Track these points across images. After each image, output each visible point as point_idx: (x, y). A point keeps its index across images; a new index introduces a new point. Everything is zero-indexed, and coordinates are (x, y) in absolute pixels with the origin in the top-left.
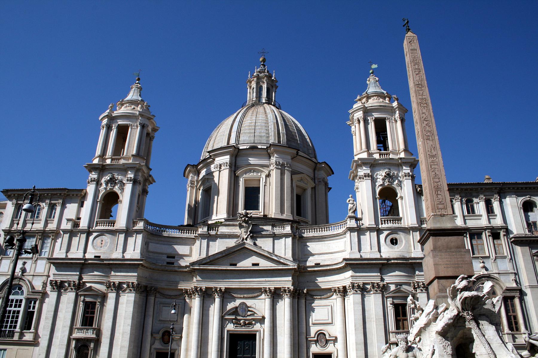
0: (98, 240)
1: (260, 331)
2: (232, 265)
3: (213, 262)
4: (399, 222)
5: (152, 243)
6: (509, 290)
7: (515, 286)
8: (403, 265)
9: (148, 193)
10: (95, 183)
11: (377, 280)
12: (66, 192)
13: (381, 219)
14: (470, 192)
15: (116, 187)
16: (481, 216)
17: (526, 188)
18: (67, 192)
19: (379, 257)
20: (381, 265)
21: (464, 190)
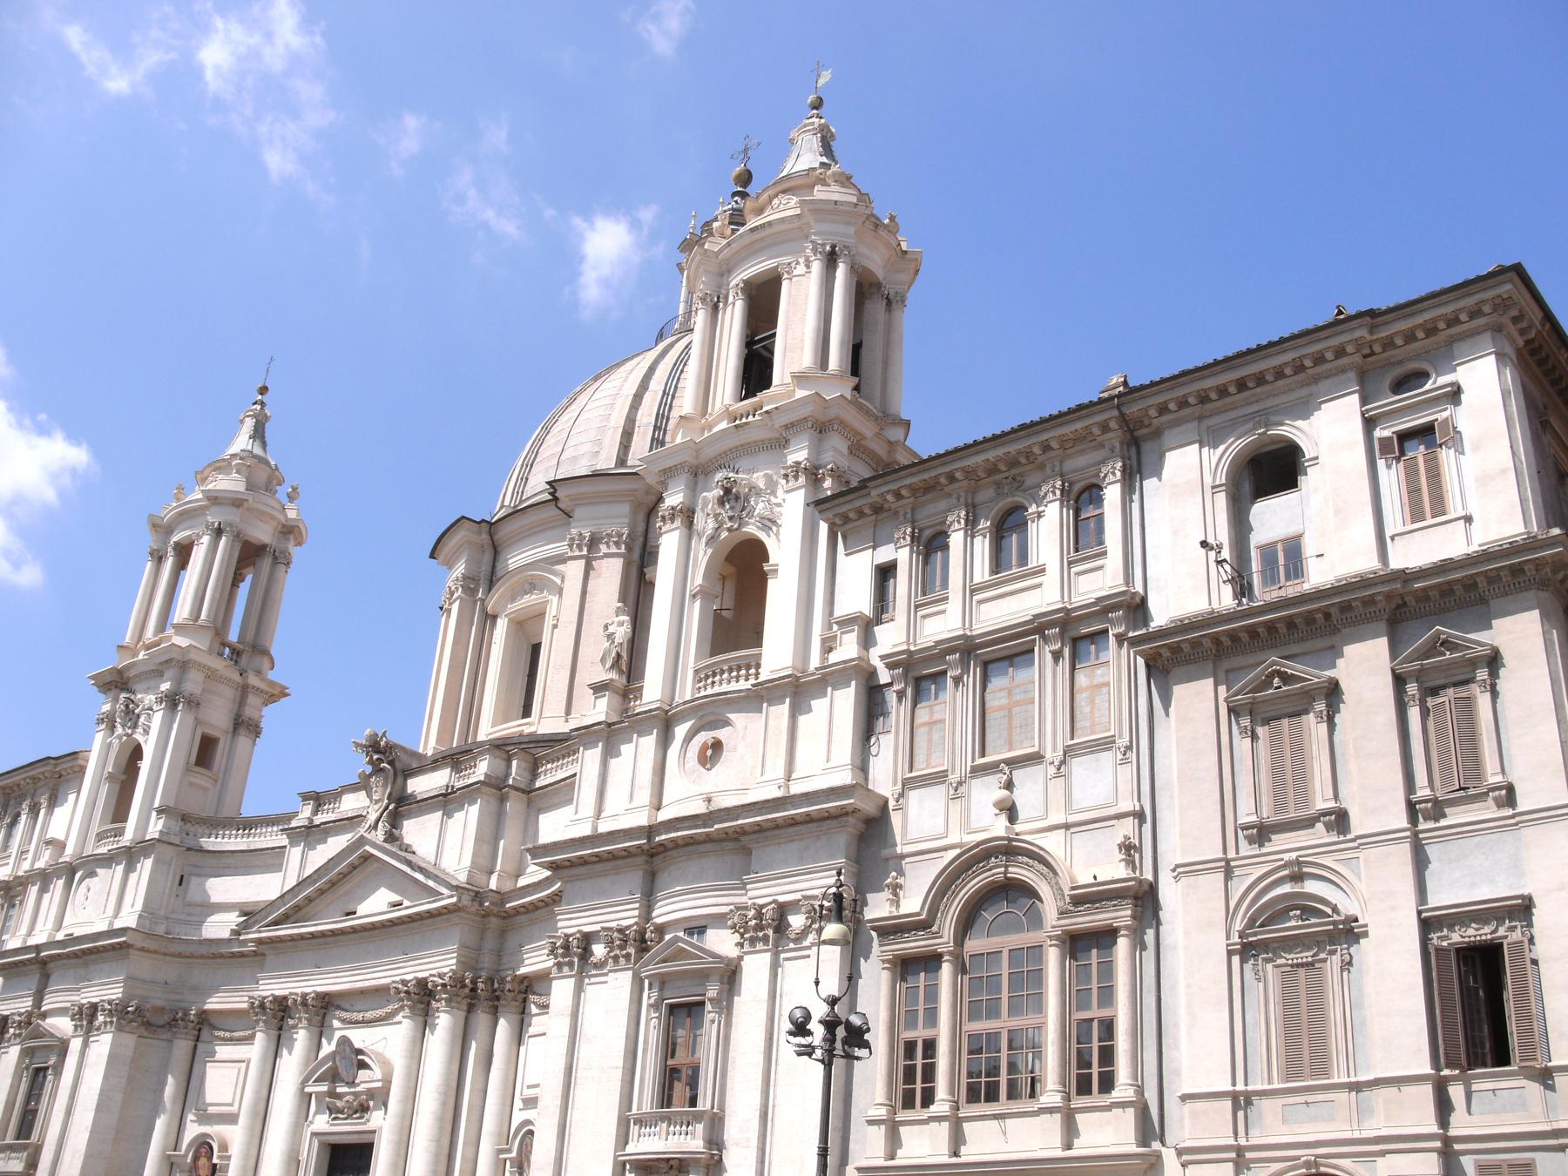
0: (84, 884)
1: (381, 1128)
2: (348, 914)
3: (300, 914)
4: (752, 671)
5: (196, 875)
6: (1085, 899)
7: (1124, 876)
8: (709, 846)
9: (257, 726)
10: (103, 726)
11: (627, 916)
12: (49, 768)
13: (696, 672)
14: (1014, 471)
15: (140, 730)
16: (1041, 571)
17: (1242, 385)
18: (56, 765)
19: (641, 819)
20: (641, 860)
21: (982, 475)
